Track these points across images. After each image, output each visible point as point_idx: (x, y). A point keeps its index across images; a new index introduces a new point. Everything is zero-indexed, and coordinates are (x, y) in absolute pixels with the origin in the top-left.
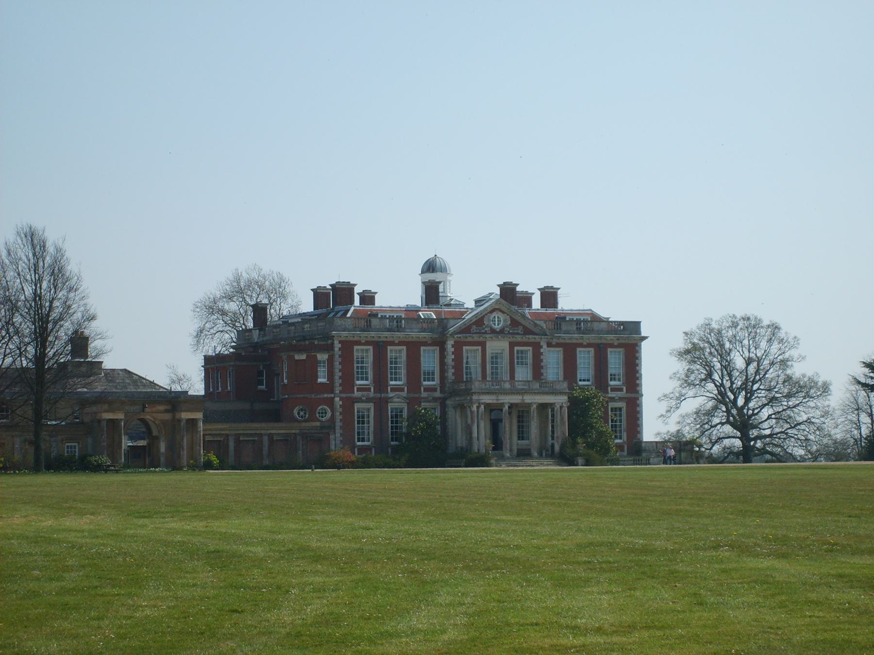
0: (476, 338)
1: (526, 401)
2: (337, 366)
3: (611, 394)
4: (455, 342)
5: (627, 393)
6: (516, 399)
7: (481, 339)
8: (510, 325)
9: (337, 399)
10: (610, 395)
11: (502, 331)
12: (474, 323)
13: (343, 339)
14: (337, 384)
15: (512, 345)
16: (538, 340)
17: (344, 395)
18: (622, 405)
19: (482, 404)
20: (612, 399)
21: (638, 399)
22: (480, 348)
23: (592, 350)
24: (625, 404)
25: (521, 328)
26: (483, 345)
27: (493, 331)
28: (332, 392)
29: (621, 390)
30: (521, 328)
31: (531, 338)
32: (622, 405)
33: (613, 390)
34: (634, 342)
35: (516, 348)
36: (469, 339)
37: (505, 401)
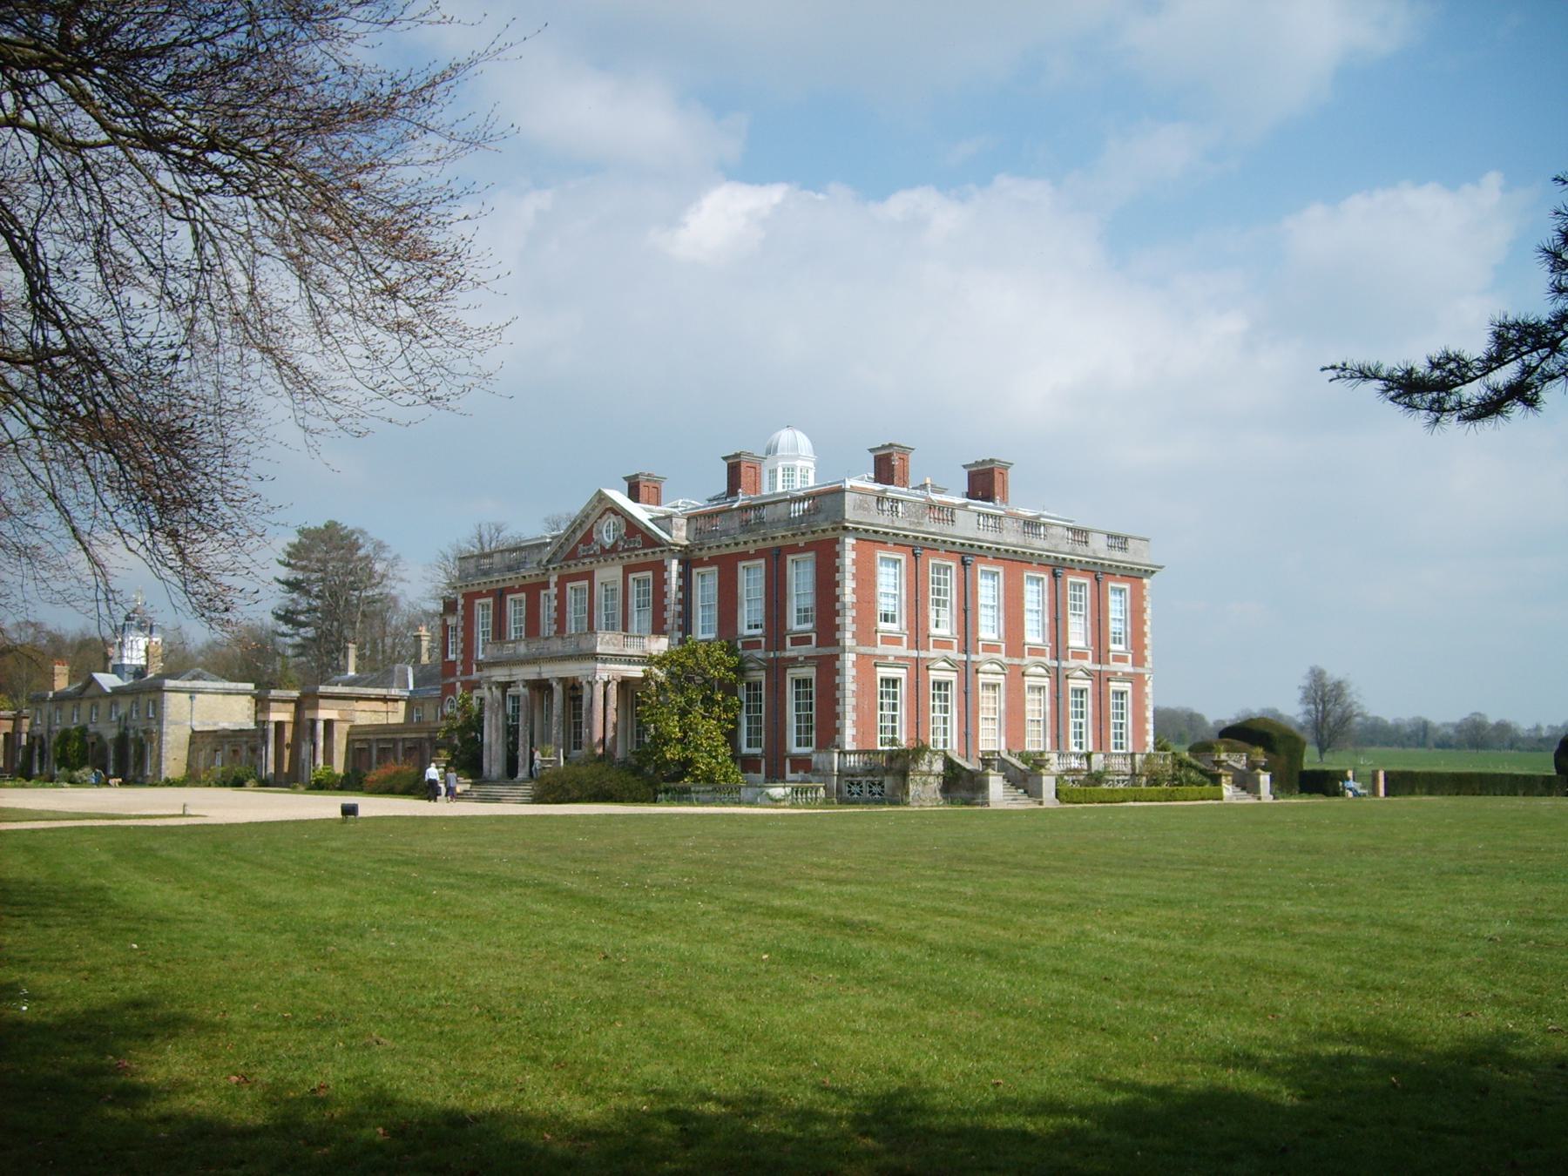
0: (581, 568)
1: (545, 676)
2: (461, 634)
3: (791, 651)
4: (559, 577)
5: (817, 646)
6: (530, 672)
7: (587, 568)
8: (625, 534)
9: (458, 684)
10: (788, 654)
11: (614, 548)
12: (580, 542)
13: (464, 591)
14: (459, 662)
15: (628, 570)
16: (658, 557)
17: (463, 678)
18: (810, 672)
19: (494, 683)
20: (793, 661)
21: (836, 657)
22: (586, 583)
23: (762, 561)
24: (814, 670)
25: (639, 538)
26: (589, 576)
27: (602, 547)
28: (454, 674)
29: (807, 640)
30: (639, 538)
31: (651, 555)
32: (810, 672)
33: (795, 642)
34: (830, 535)
35: (631, 576)
36: (573, 570)
37: (520, 677)
